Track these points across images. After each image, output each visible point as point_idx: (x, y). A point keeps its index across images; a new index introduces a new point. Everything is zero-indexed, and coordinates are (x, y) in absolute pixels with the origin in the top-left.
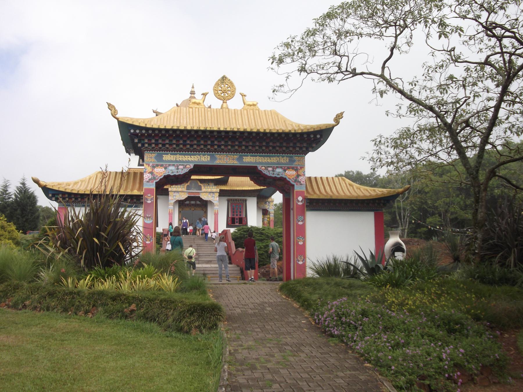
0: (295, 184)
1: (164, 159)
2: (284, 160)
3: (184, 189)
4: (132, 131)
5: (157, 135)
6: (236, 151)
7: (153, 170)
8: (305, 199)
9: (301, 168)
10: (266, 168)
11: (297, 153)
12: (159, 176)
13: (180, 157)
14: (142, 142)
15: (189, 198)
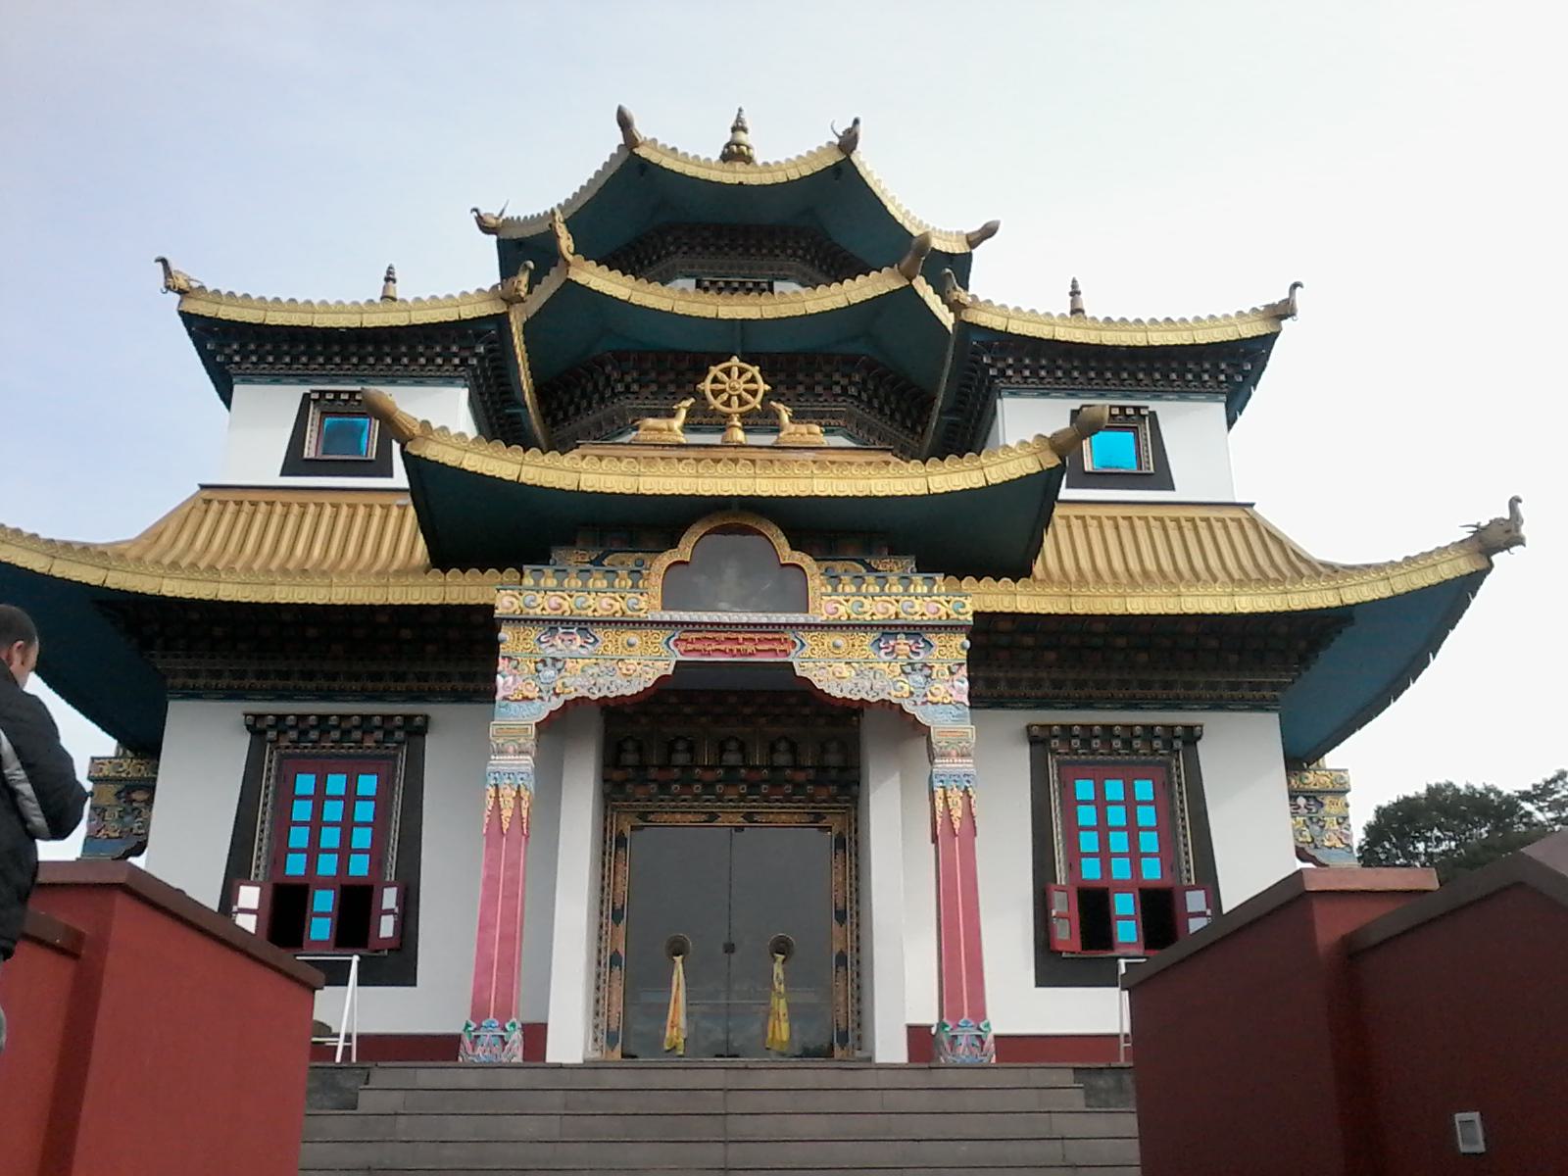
3: (648, 604)
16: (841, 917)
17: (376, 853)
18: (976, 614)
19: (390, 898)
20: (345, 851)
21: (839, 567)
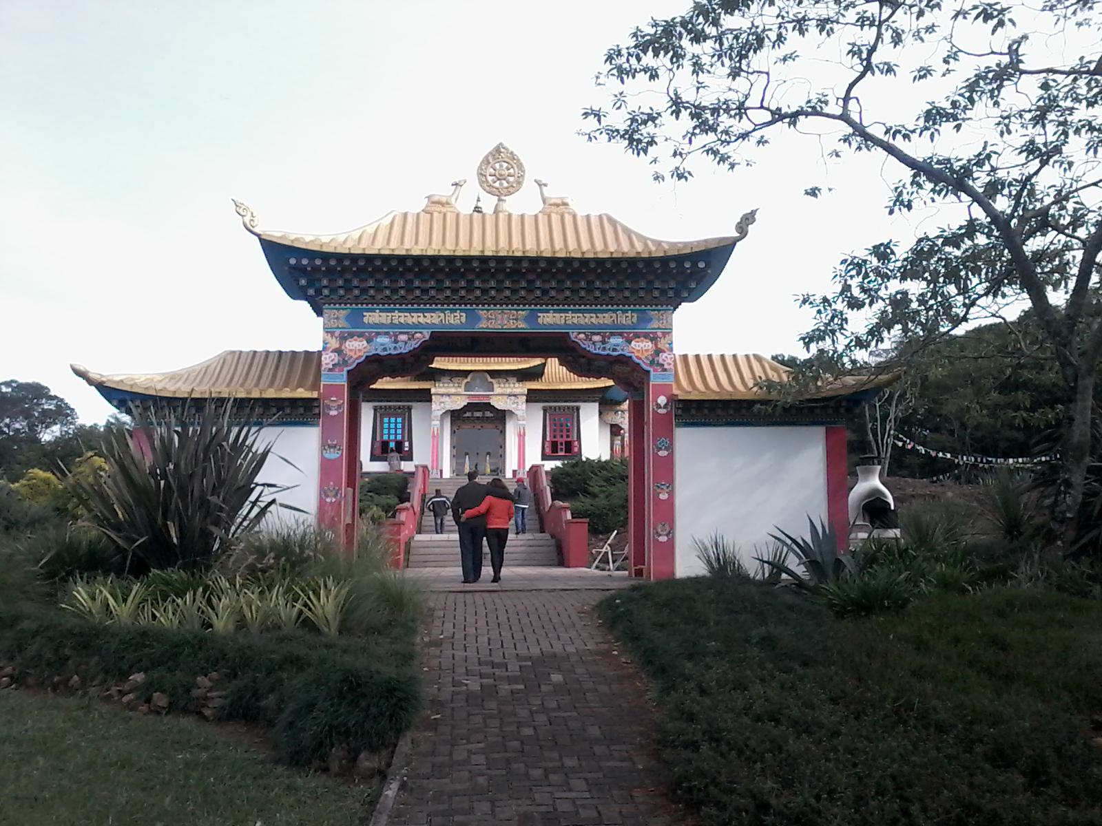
0: (651, 369)
1: (365, 320)
2: (626, 318)
3: (461, 390)
4: (293, 261)
5: (345, 270)
6: (523, 301)
7: (341, 345)
8: (672, 400)
9: (664, 334)
10: (588, 338)
11: (655, 302)
12: (355, 357)
13: (400, 317)
14: (317, 285)
15: (470, 407)
16: (501, 447)
17: (403, 434)
18: (529, 390)
19: (407, 444)
20: (396, 434)
21: (500, 380)
